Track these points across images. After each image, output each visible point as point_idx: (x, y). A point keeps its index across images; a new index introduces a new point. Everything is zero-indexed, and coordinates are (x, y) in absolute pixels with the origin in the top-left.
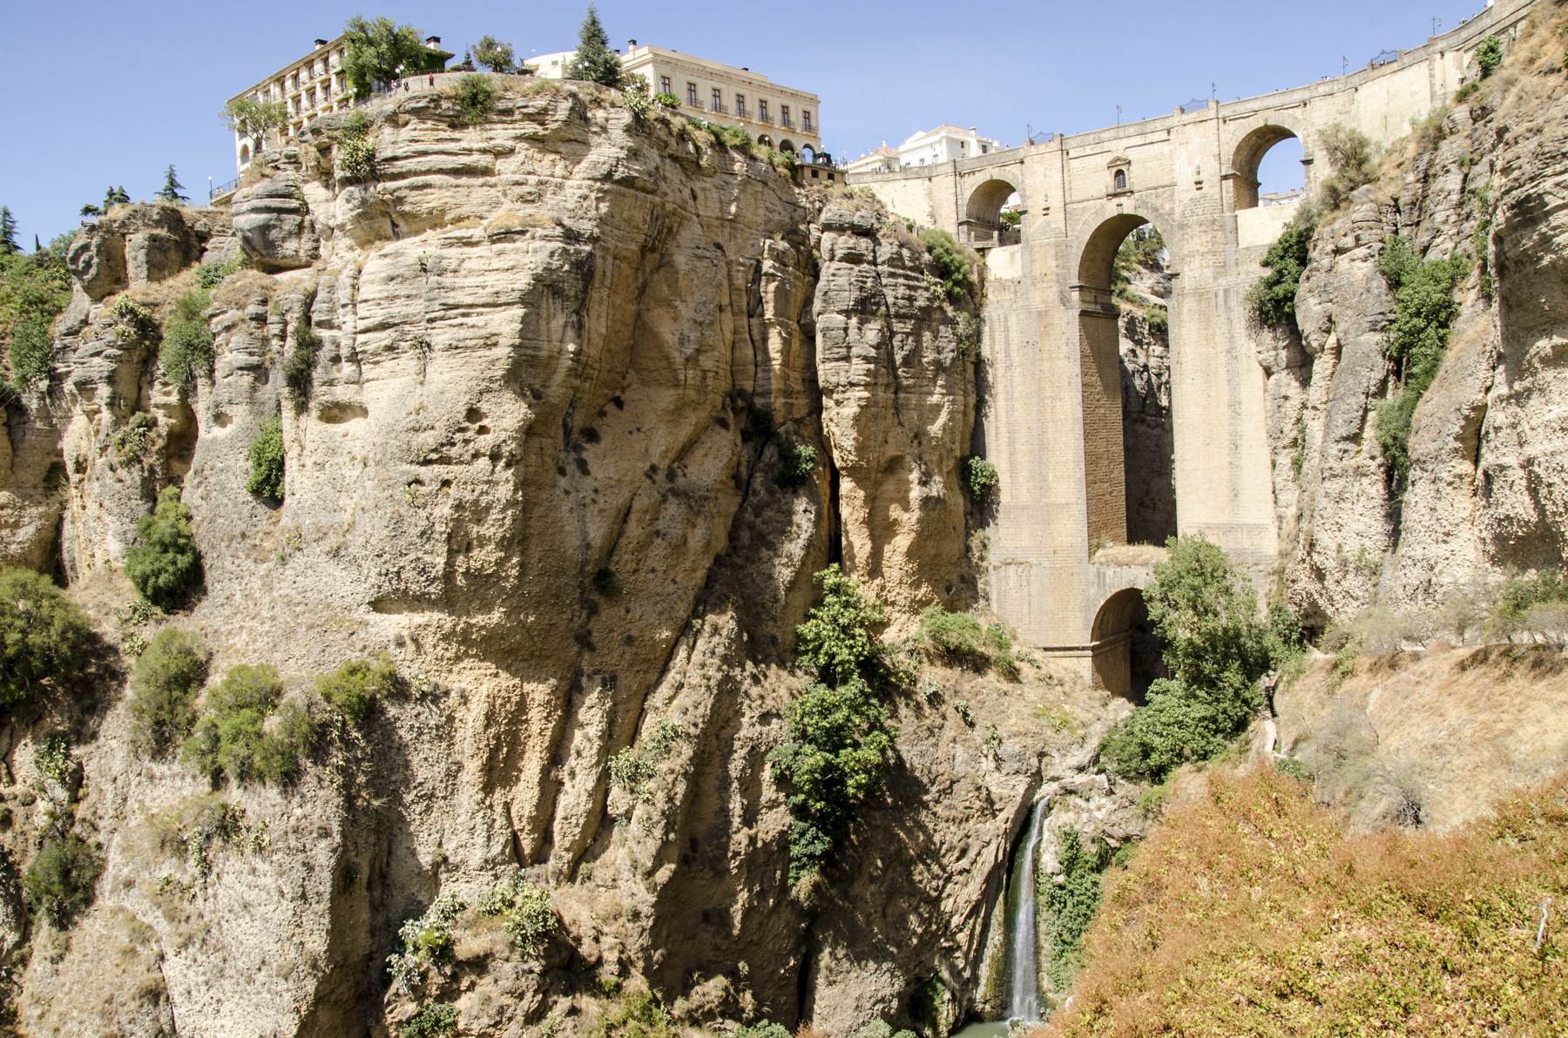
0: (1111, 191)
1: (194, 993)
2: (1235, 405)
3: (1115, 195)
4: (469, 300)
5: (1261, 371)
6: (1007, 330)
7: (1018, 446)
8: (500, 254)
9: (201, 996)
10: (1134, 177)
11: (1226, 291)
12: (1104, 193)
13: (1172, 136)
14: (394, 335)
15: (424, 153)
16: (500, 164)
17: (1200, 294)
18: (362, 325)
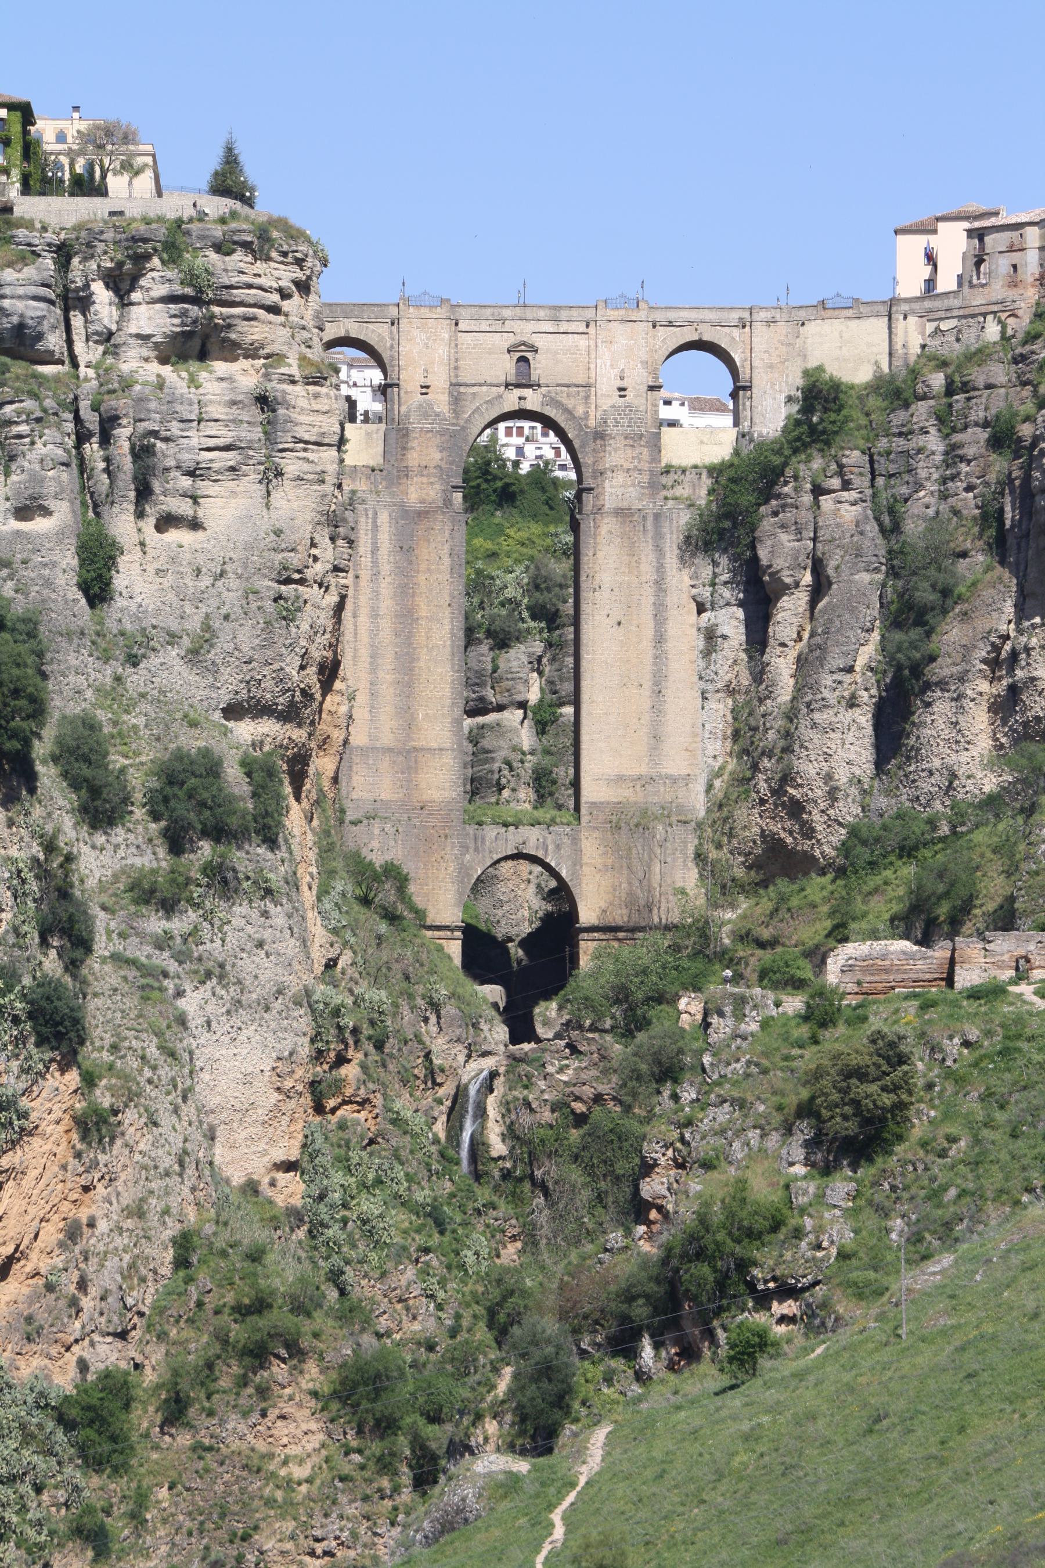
0: (512, 379)
1: (214, 1024)
2: (660, 639)
3: (518, 386)
4: (307, 437)
5: (693, 607)
6: (375, 528)
7: (381, 674)
8: (317, 396)
9: (221, 1027)
10: (540, 367)
11: (657, 517)
12: (502, 379)
13: (592, 330)
14: (239, 458)
15: (250, 286)
16: (286, 306)
17: (622, 513)
18: (212, 442)
